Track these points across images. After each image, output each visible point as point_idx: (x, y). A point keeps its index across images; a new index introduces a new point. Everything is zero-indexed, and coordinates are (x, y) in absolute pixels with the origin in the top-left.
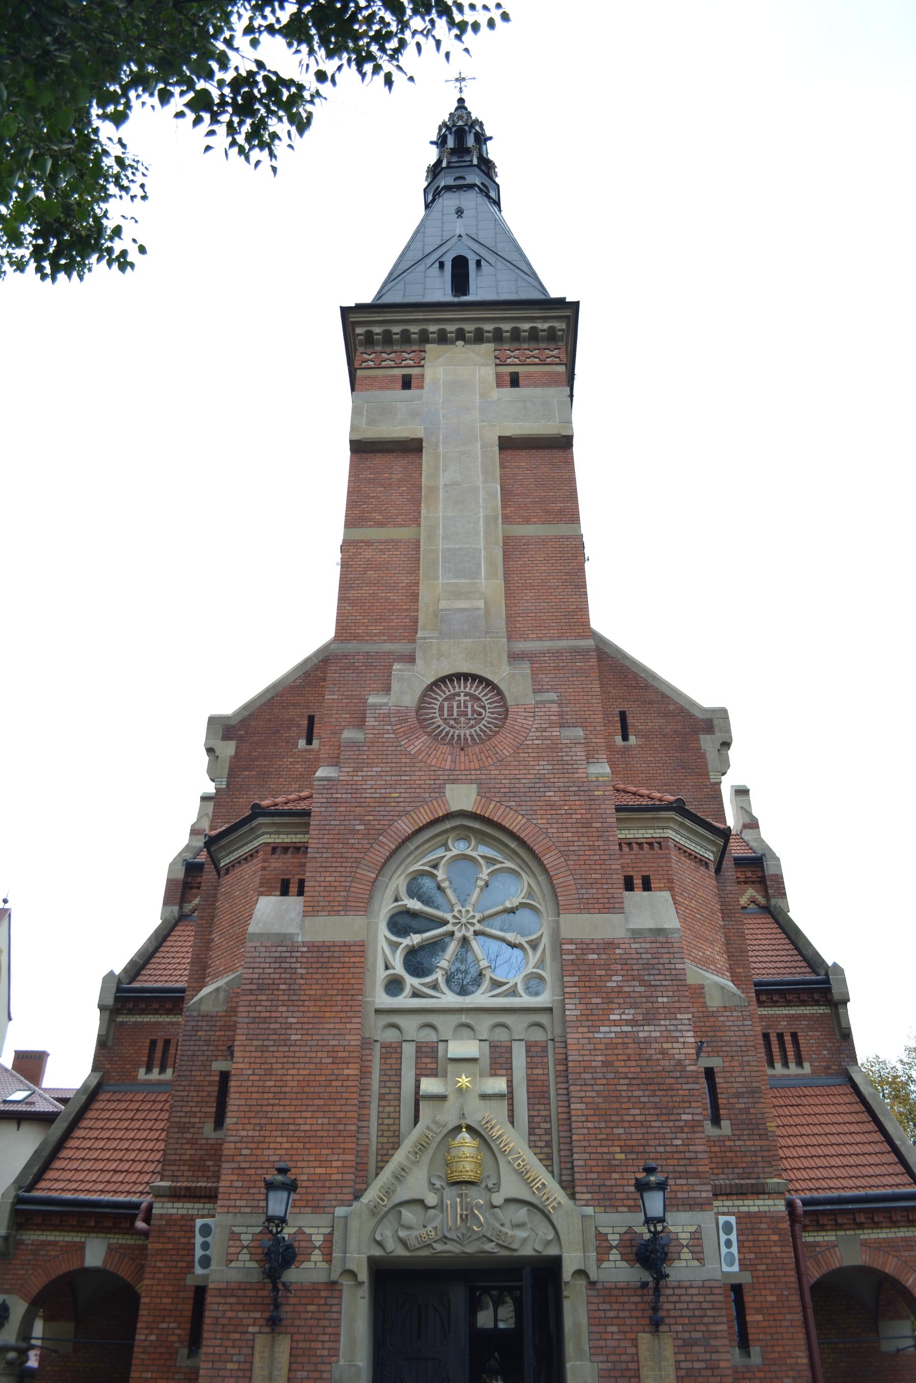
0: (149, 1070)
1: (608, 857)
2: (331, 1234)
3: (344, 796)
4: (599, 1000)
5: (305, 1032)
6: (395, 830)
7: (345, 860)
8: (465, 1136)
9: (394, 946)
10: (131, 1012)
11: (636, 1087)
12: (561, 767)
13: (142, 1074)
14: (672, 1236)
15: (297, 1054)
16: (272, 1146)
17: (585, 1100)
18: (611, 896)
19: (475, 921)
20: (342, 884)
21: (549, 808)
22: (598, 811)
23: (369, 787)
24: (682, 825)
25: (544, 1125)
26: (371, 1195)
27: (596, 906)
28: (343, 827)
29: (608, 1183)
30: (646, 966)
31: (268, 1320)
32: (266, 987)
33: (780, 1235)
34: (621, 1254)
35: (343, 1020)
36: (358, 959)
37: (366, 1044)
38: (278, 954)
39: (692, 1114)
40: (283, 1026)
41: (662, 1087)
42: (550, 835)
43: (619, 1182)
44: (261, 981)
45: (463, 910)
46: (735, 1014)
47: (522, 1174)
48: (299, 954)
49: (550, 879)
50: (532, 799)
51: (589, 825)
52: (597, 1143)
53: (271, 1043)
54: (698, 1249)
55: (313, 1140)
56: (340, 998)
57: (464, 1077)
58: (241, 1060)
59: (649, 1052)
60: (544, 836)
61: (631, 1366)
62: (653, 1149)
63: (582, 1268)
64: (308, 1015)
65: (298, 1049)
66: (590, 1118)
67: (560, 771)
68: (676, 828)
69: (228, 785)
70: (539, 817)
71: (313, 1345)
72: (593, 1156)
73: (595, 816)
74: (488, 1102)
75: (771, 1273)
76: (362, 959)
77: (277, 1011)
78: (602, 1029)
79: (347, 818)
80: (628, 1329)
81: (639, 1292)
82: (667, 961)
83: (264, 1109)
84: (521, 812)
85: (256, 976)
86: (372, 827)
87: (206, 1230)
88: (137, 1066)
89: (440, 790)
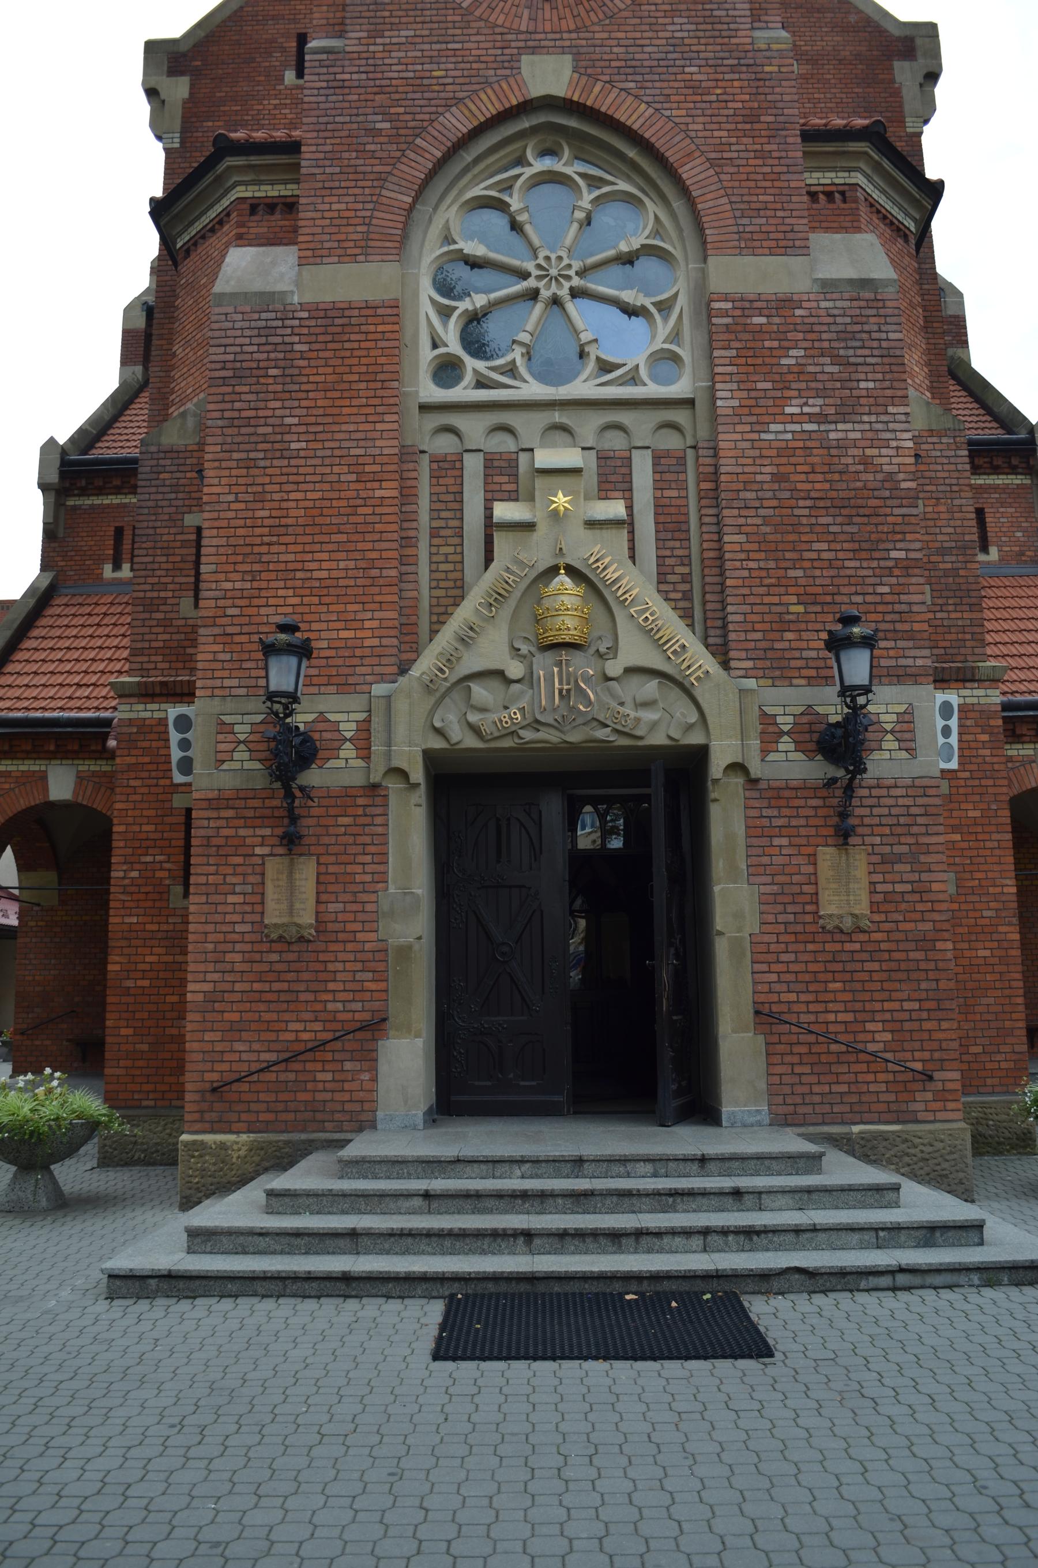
0: (117, 567)
1: (785, 169)
2: (368, 721)
3: (355, 76)
4: (768, 385)
5: (311, 437)
6: (441, 128)
7: (361, 176)
8: (563, 579)
9: (445, 313)
10: (84, 492)
11: (823, 512)
12: (709, 27)
13: (107, 571)
14: (874, 718)
15: (302, 470)
16: (271, 601)
17: (744, 529)
18: (788, 228)
19: (572, 273)
20: (359, 214)
21: (691, 91)
22: (769, 98)
23: (395, 61)
24: (877, 167)
25: (679, 570)
26: (425, 664)
27: (765, 244)
28: (355, 126)
29: (777, 645)
30: (843, 335)
31: (282, 838)
32: (248, 373)
33: (991, 734)
34: (795, 742)
35: (371, 418)
36: (389, 328)
37: (408, 455)
38: (263, 324)
39: (907, 550)
40: (278, 429)
41: (862, 511)
42: (693, 134)
43: (794, 645)
44: (238, 365)
45: (553, 256)
46: (944, 440)
47: (651, 634)
48: (296, 322)
49: (691, 203)
50: (663, 77)
51: (755, 119)
52: (762, 590)
53: (261, 455)
54: (907, 736)
55: (332, 591)
56: (363, 385)
57: (560, 495)
58: (216, 481)
59: (843, 460)
60: (682, 135)
61: (806, 889)
62: (846, 599)
63: (740, 760)
64: (315, 412)
65: (302, 462)
66: (752, 555)
67: (707, 34)
68: (869, 171)
69: (182, 142)
70: (675, 105)
71: (349, 869)
72: (756, 609)
73: (765, 105)
74: (598, 532)
75: (976, 782)
76: (396, 327)
77: (266, 408)
78: (773, 427)
79: (361, 111)
80: (804, 841)
81: (824, 793)
82: (876, 328)
83: (256, 549)
84: (645, 99)
85: (231, 357)
86: (403, 124)
87: (184, 723)
88: (100, 561)
89: (512, 65)
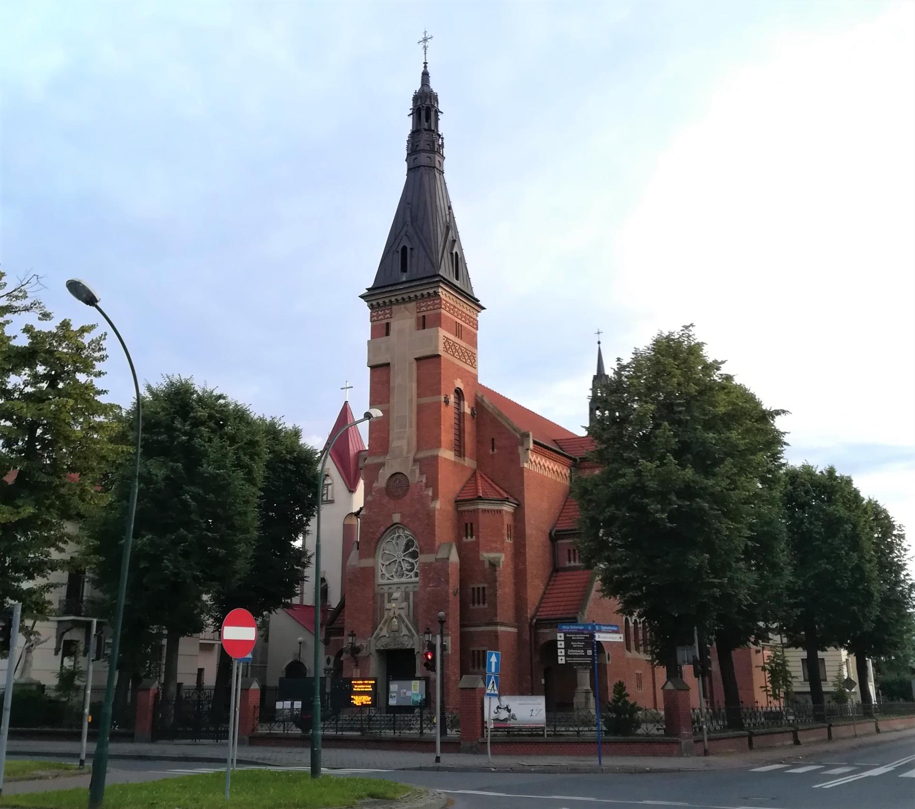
8: (395, 620)
26: (374, 635)
